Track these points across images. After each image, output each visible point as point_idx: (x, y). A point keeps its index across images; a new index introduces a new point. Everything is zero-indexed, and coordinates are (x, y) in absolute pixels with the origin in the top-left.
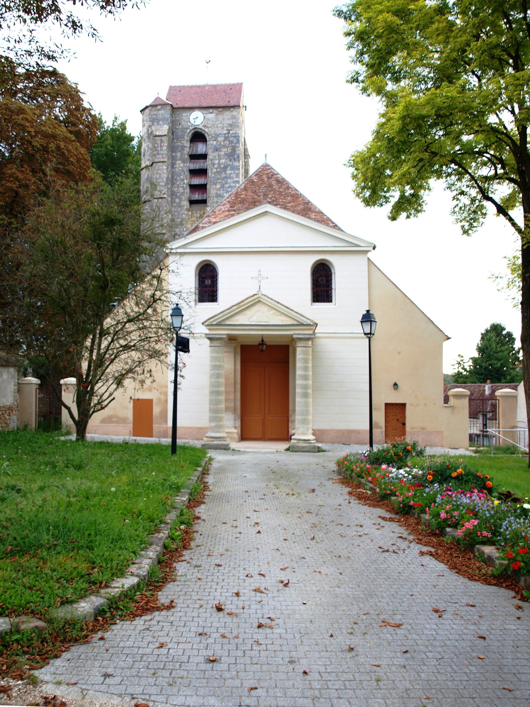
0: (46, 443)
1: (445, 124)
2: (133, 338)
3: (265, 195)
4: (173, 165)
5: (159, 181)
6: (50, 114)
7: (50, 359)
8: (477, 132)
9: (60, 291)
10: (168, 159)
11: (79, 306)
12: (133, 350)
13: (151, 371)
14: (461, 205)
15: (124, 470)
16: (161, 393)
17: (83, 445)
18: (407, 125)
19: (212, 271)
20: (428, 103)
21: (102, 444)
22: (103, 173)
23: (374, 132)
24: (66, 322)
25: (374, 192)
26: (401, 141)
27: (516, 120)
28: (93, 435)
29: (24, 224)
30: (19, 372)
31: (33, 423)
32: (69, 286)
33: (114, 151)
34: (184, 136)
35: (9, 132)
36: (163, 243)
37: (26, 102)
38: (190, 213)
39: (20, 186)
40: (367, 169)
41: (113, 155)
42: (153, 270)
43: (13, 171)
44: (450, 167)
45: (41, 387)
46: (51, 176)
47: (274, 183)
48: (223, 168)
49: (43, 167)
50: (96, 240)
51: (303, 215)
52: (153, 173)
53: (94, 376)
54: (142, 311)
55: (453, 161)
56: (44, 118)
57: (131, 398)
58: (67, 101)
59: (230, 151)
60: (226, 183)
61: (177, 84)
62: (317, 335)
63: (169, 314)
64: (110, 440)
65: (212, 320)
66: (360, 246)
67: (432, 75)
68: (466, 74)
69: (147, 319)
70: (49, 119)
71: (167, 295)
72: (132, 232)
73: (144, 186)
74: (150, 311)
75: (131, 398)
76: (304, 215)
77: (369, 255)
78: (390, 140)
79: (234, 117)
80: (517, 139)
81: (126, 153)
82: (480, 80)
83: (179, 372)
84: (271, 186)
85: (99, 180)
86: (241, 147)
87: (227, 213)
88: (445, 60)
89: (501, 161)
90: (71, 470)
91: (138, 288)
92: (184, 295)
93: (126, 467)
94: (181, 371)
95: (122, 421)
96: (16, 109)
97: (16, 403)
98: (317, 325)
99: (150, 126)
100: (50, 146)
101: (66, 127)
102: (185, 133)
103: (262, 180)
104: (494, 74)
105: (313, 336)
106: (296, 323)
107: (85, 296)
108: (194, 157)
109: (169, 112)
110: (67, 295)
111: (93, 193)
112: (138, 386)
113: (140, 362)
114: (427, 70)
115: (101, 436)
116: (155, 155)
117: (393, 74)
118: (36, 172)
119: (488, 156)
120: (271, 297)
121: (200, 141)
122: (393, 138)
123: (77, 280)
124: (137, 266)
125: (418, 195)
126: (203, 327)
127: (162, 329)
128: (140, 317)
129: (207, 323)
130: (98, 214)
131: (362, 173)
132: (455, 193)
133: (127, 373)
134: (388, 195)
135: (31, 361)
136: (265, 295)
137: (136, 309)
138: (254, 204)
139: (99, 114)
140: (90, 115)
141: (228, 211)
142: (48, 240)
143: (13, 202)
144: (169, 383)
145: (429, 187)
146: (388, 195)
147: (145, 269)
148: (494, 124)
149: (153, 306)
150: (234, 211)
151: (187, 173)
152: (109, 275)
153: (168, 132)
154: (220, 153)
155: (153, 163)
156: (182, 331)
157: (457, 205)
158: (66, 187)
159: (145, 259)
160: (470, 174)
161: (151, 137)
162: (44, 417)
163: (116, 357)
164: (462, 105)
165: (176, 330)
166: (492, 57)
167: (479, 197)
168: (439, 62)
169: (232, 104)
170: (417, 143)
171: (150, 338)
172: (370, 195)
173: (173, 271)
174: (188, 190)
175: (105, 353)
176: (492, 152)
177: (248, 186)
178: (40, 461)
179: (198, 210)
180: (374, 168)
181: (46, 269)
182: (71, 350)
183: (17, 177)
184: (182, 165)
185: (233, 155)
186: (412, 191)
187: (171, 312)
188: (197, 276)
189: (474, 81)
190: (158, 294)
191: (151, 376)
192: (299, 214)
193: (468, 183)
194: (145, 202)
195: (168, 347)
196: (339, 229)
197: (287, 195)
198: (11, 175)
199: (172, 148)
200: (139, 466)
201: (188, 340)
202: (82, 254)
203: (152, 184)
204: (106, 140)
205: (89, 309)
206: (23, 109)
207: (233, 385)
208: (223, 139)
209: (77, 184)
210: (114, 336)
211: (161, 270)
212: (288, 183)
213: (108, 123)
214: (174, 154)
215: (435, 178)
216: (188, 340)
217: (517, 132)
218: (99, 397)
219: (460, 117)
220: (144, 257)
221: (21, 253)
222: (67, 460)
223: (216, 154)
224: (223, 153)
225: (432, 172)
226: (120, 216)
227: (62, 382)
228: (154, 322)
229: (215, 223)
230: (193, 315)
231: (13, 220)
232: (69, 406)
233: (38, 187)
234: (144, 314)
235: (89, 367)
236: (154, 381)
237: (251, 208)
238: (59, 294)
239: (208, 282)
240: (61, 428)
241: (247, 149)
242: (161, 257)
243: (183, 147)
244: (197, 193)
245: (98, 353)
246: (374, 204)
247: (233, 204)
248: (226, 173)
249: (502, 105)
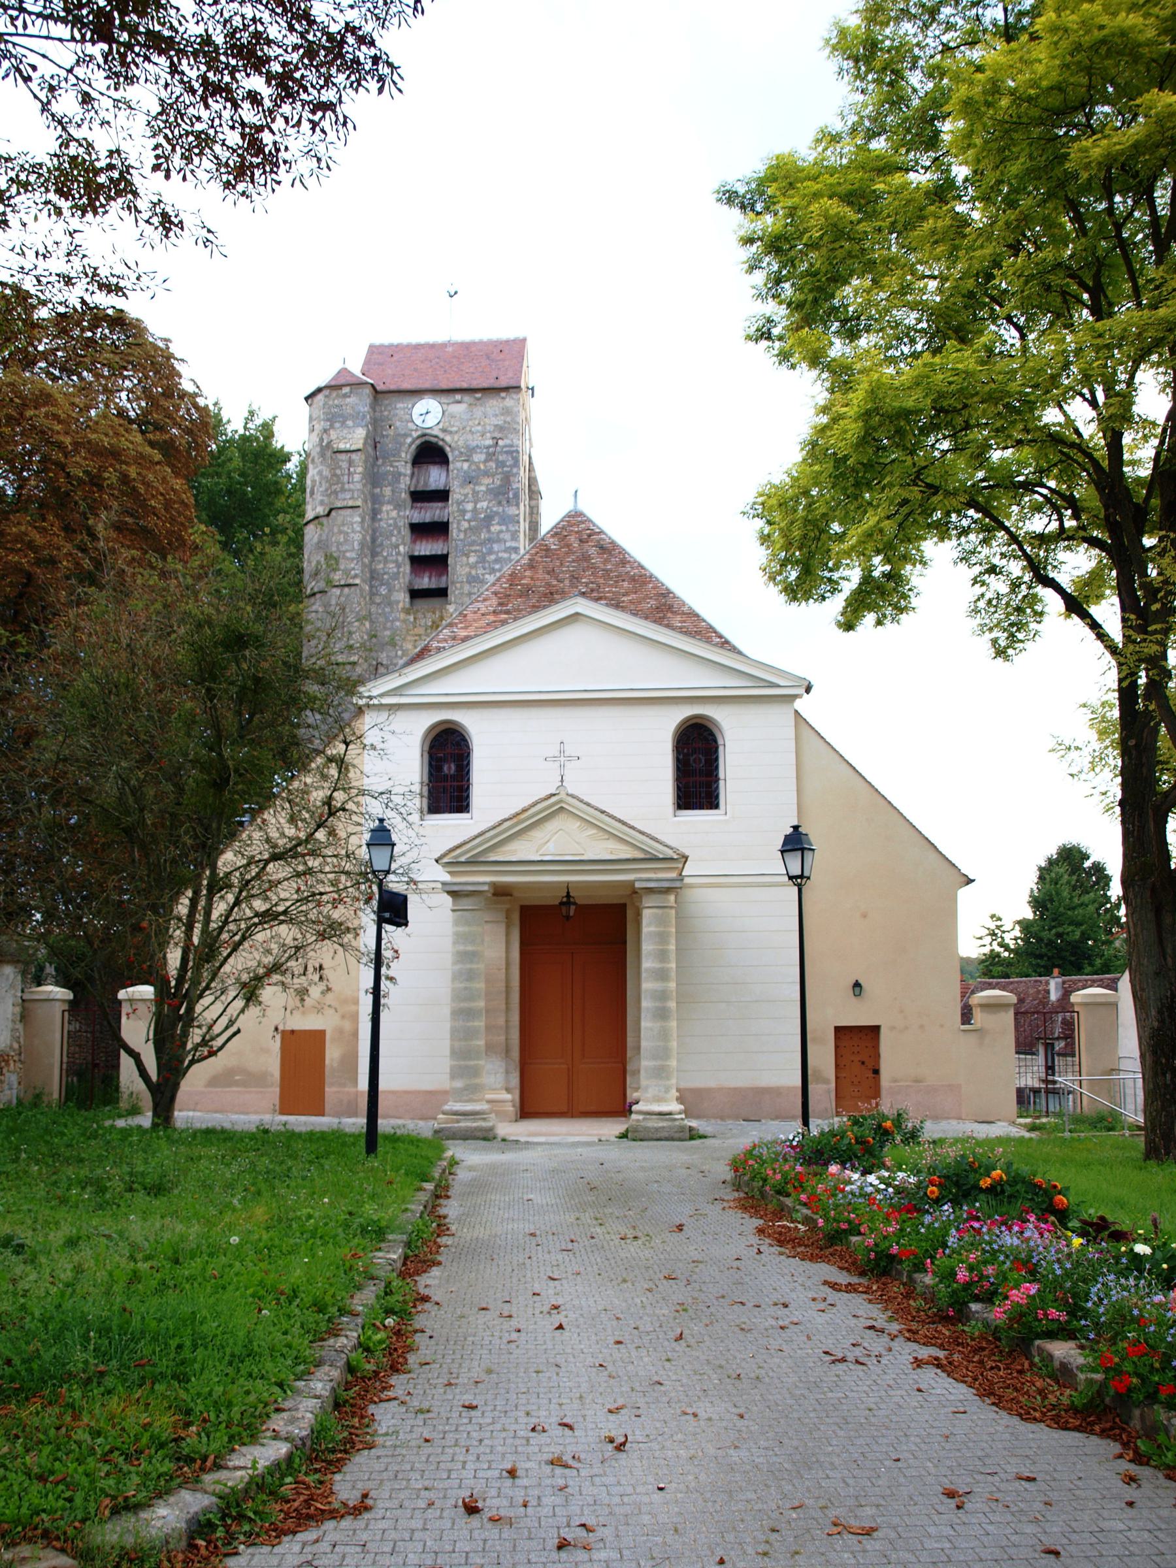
0: (83, 1135)
1: (954, 427)
2: (283, 895)
3: (575, 579)
4: (375, 514)
5: (343, 548)
6: (107, 406)
7: (96, 943)
8: (1019, 442)
9: (122, 794)
10: (365, 501)
11: (163, 826)
12: (282, 922)
13: (321, 967)
14: (988, 595)
15: (259, 1193)
16: (343, 1017)
17: (168, 1138)
18: (875, 429)
19: (458, 744)
20: (918, 385)
21: (210, 1135)
22: (222, 531)
23: (804, 444)
24: (133, 861)
25: (807, 571)
26: (862, 464)
27: (1101, 419)
28: (191, 1114)
29: (43, 643)
30: (24, 973)
31: (55, 1089)
32: (142, 782)
33: (246, 484)
34: (399, 451)
35: (16, 444)
36: (351, 686)
37: (55, 379)
38: (411, 618)
39: (38, 562)
40: (792, 523)
41: (245, 493)
42: (330, 739)
43: (23, 528)
44: (966, 516)
45: (74, 1007)
46: (107, 540)
47: (593, 551)
49: (90, 522)
50: (204, 680)
51: (655, 622)
52: (331, 530)
53: (195, 982)
54: (302, 835)
55: (972, 504)
56: (93, 412)
57: (276, 1029)
58: (147, 377)
59: (499, 483)
60: (491, 552)
61: (386, 341)
62: (687, 880)
63: (364, 842)
64: (227, 1126)
65: (458, 851)
66: (779, 686)
67: (924, 325)
68: (994, 322)
69: (313, 853)
70: (104, 416)
71: (360, 798)
72: (284, 663)
73: (311, 559)
74: (321, 835)
75: (276, 1029)
76: (658, 621)
77: (798, 704)
78: (840, 461)
79: (507, 411)
80: (1103, 457)
81: (272, 489)
82: (1023, 337)
83: (384, 970)
84: (586, 558)
85: (213, 549)
86: (523, 475)
87: (492, 618)
88: (952, 295)
89: (1071, 502)
90: (141, 1198)
91: (296, 784)
92: (397, 799)
93: (263, 1187)
94: (389, 967)
95: (256, 1079)
96: (32, 394)
97: (16, 1046)
98: (686, 858)
99: (325, 431)
100: (106, 475)
101: (143, 432)
102: (402, 444)
103: (568, 546)
104: (1051, 324)
105: (678, 884)
106: (641, 855)
107: (179, 804)
108: (420, 497)
110: (136, 803)
111: (199, 578)
112: (293, 1001)
113: (298, 948)
114: (914, 315)
115: (207, 1116)
116: (336, 493)
117: (844, 322)
118: (74, 531)
119: (1044, 491)
120: (586, 799)
121: (434, 463)
122: (846, 458)
123: (159, 769)
124: (295, 736)
125: (900, 576)
126: (439, 867)
127: (347, 873)
128: (299, 849)
129: (446, 860)
130: (209, 622)
131: (781, 530)
132: (977, 569)
133: (268, 973)
134: (836, 576)
135: (54, 952)
136: (573, 796)
137: (291, 831)
138: (551, 597)
139: (216, 404)
140: (196, 406)
141: (494, 612)
142: (96, 681)
143: (21, 595)
144: (362, 993)
145: (922, 557)
146: (836, 576)
147: (311, 742)
148: (1054, 425)
149: (328, 824)
150: (508, 612)
151: (406, 532)
152: (232, 758)
153: (364, 444)
154: (477, 488)
155: (331, 510)
156: (391, 877)
157: (983, 595)
158: (141, 566)
159: (310, 721)
160: (1007, 530)
161: (329, 454)
162: (80, 1074)
163: (244, 938)
164: (987, 388)
165: (379, 876)
166: (1048, 288)
167: (1027, 577)
168: (938, 299)
169: (503, 383)
170: (895, 465)
171: (321, 894)
172: (798, 578)
173: (373, 747)
174: (407, 568)
175: (221, 929)
176: (1052, 484)
177: (538, 558)
178: (69, 1179)
179: (427, 609)
180: (806, 521)
181: (92, 745)
182: (145, 924)
183: (31, 542)
184: (394, 514)
185: (504, 492)
186: (888, 568)
187: (367, 836)
188: (426, 756)
189: (1011, 335)
190: (339, 796)
191: (321, 978)
192: (646, 618)
193: (1004, 549)
194: (314, 594)
195: (360, 914)
196: (734, 650)
197: (620, 578)
198: (18, 538)
199: (374, 478)
200: (293, 1184)
201: (405, 898)
202: (170, 711)
203: (328, 557)
204: (230, 460)
205: (186, 833)
206: (49, 396)
207: (504, 995)
208: (483, 457)
209: (164, 558)
210: (241, 892)
211: (347, 744)
212: (623, 552)
213: (235, 424)
214: (378, 490)
215: (935, 539)
216: (404, 899)
217: (1102, 442)
218: (204, 1029)
219: (984, 411)
220: (311, 717)
221: (37, 709)
222: (131, 1174)
223: (468, 490)
224: (483, 488)
225: (929, 526)
226: (259, 628)
227: (122, 994)
228: (329, 860)
229: (465, 639)
230: (417, 842)
231: (19, 637)
232: (137, 1050)
233: (78, 564)
234: (307, 841)
235: (184, 960)
236: (329, 989)
237: (545, 607)
238: (120, 799)
239: (450, 768)
240: (117, 1100)
241: (535, 479)
242: (346, 716)
243: (397, 476)
244: (427, 575)
245: (205, 931)
246: (807, 596)
247: (504, 599)
248: (489, 531)
249: (1071, 389)
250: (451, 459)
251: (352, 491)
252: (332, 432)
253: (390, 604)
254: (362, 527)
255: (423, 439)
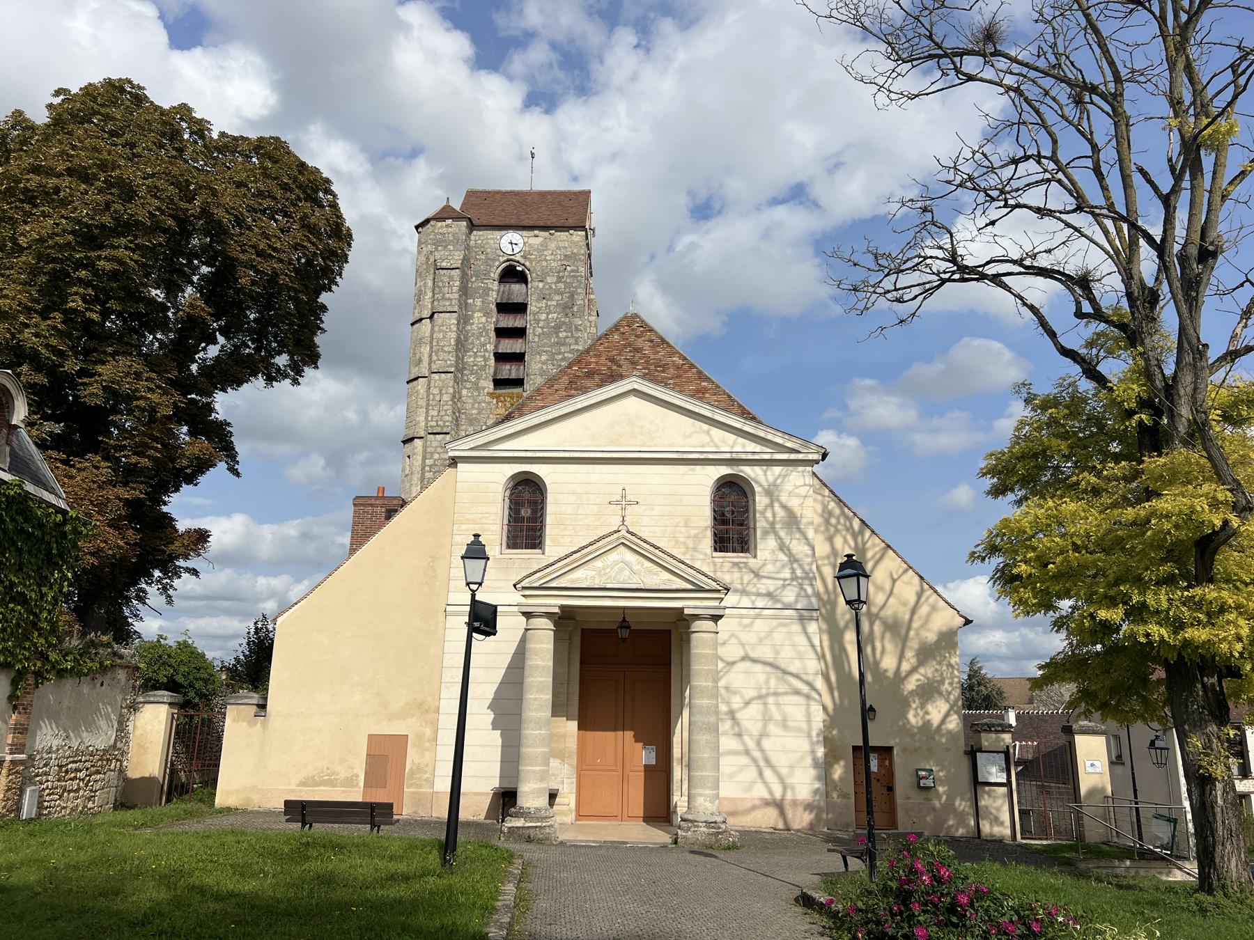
48: (553, 327)
108: (504, 308)
109: (464, 229)
151: (493, 334)
155: (433, 313)
174: (492, 361)
184: (484, 320)
208: (555, 279)
223: (544, 303)
243: (487, 291)
248: (558, 336)
250: (529, 279)
251: (450, 299)
252: (436, 253)
253: (478, 389)
254: (458, 328)
255: (508, 263)
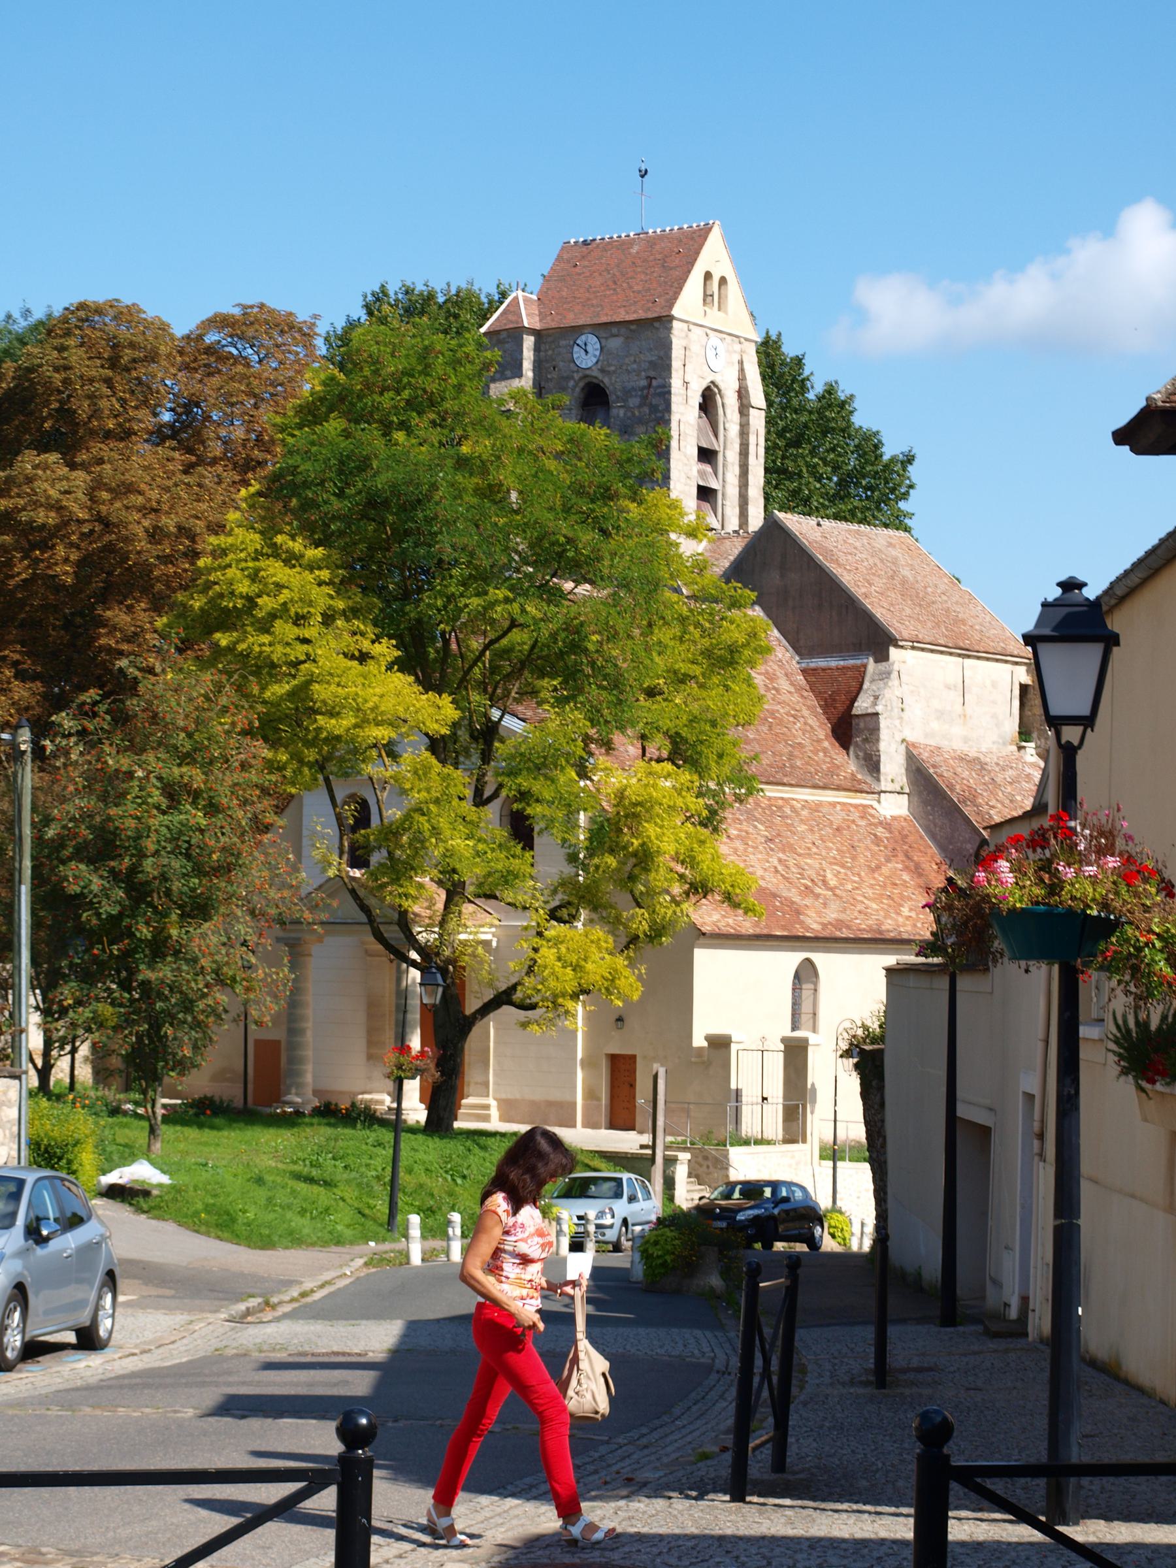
255: (587, 380)
